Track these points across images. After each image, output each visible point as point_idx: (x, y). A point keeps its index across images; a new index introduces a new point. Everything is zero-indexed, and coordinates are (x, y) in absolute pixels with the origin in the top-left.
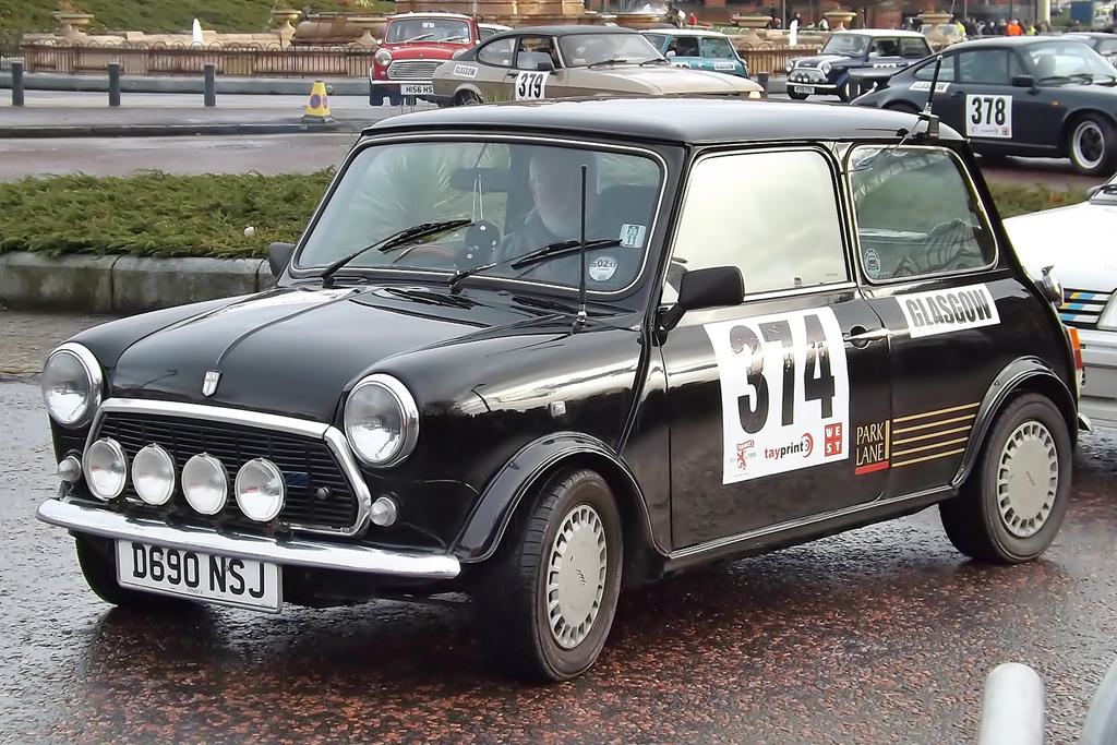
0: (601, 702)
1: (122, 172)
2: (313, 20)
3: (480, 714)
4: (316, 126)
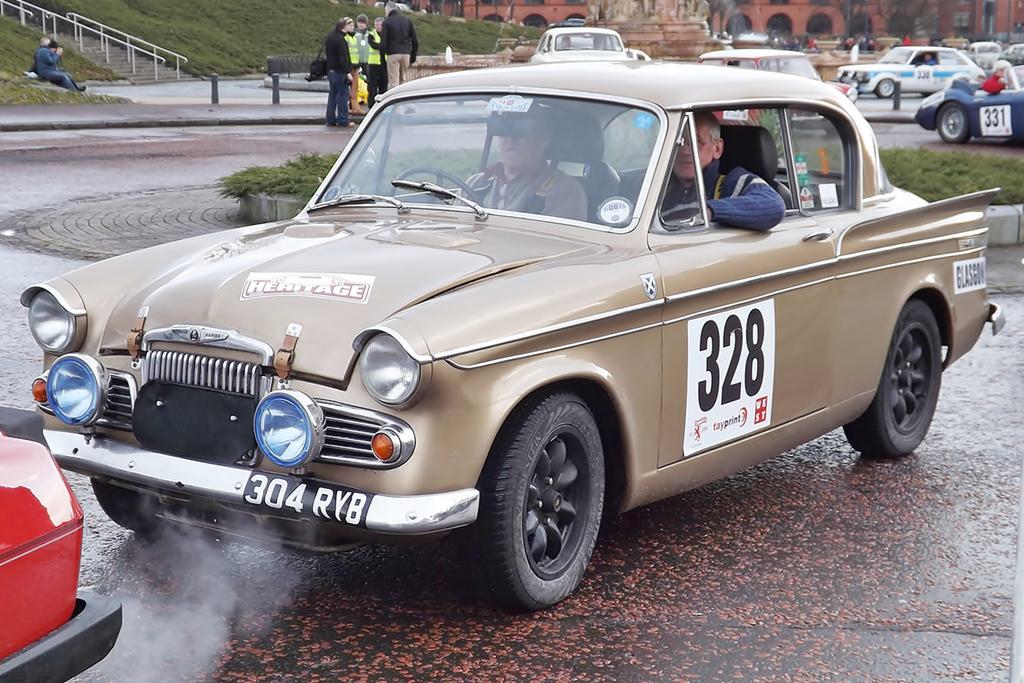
2: (525, 45)
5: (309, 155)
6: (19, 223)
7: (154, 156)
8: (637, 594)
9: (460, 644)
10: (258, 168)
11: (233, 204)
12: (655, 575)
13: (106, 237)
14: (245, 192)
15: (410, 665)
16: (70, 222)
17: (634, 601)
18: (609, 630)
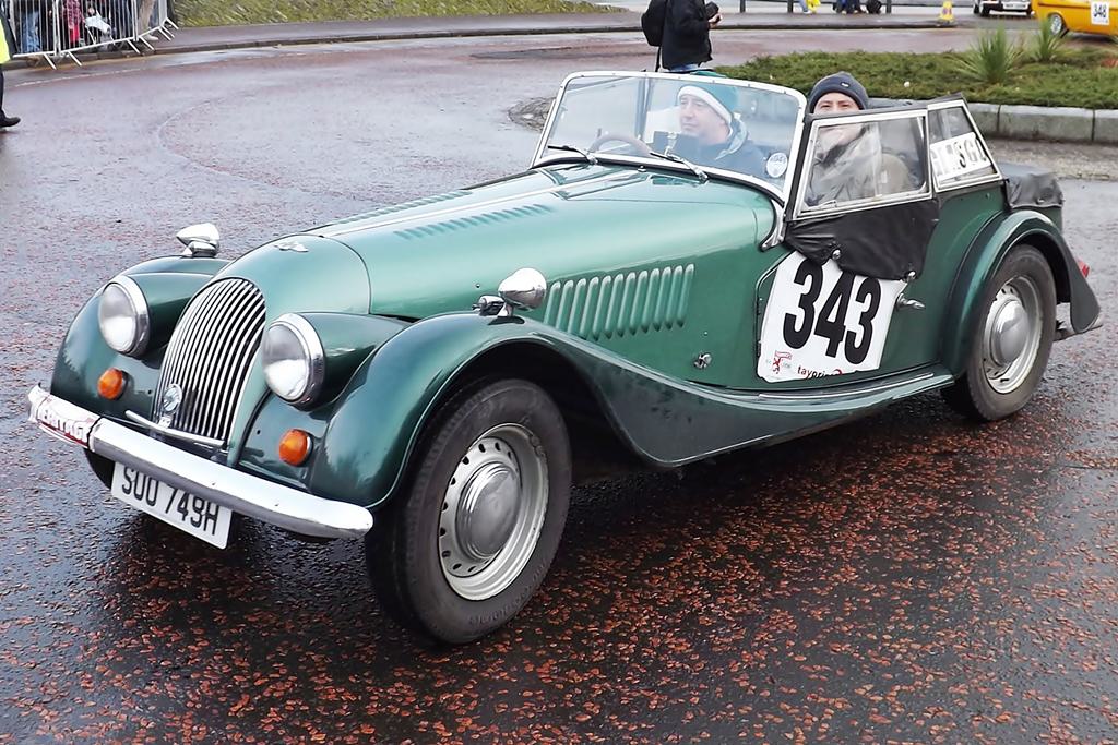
1: (842, 50)
4: (945, 25)
5: (764, 55)
8: (999, 435)
9: (850, 471)
15: (809, 486)
17: (996, 441)
18: (973, 465)
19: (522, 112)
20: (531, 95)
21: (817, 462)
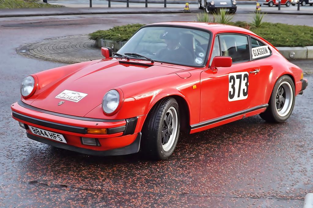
0: (237, 147)
3: (213, 148)
5: (116, 25)
6: (28, 48)
7: (71, 24)
9: (147, 203)
10: (101, 31)
11: (93, 42)
12: (211, 177)
13: (53, 52)
14: (96, 38)
16: (43, 47)
17: (204, 188)
19: (22, 49)
20: (25, 42)
21: (134, 200)
